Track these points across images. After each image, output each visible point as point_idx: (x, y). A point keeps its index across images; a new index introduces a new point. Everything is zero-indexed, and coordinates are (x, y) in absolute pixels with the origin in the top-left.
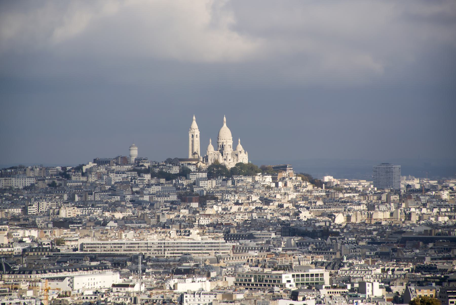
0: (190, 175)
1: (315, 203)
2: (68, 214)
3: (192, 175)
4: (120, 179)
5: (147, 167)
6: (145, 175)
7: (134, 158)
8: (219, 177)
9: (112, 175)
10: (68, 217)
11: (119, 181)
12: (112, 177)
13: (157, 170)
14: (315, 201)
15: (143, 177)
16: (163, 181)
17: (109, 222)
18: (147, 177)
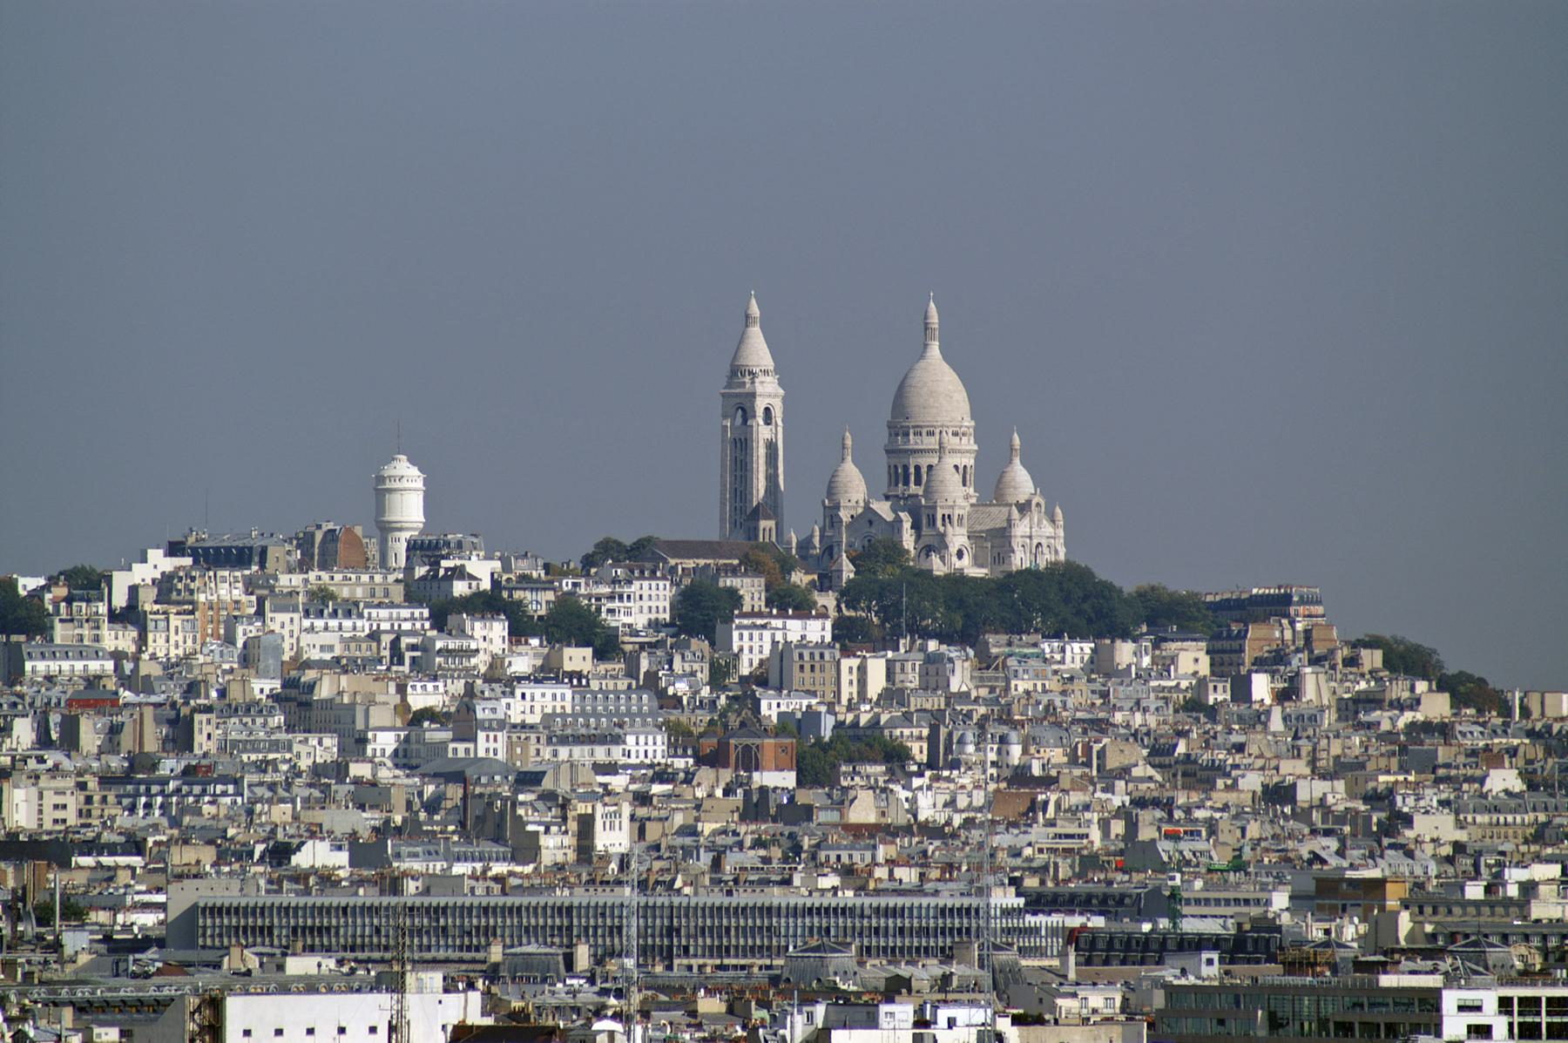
0: (736, 634)
1: (1482, 781)
2: (49, 815)
3: (746, 633)
4: (331, 648)
5: (486, 585)
6: (478, 625)
7: (407, 535)
8: (903, 643)
9: (279, 621)
10: (48, 825)
11: (327, 656)
12: (286, 632)
13: (538, 603)
14: (1478, 773)
15: (462, 633)
16: (577, 658)
17: (298, 848)
18: (490, 635)
